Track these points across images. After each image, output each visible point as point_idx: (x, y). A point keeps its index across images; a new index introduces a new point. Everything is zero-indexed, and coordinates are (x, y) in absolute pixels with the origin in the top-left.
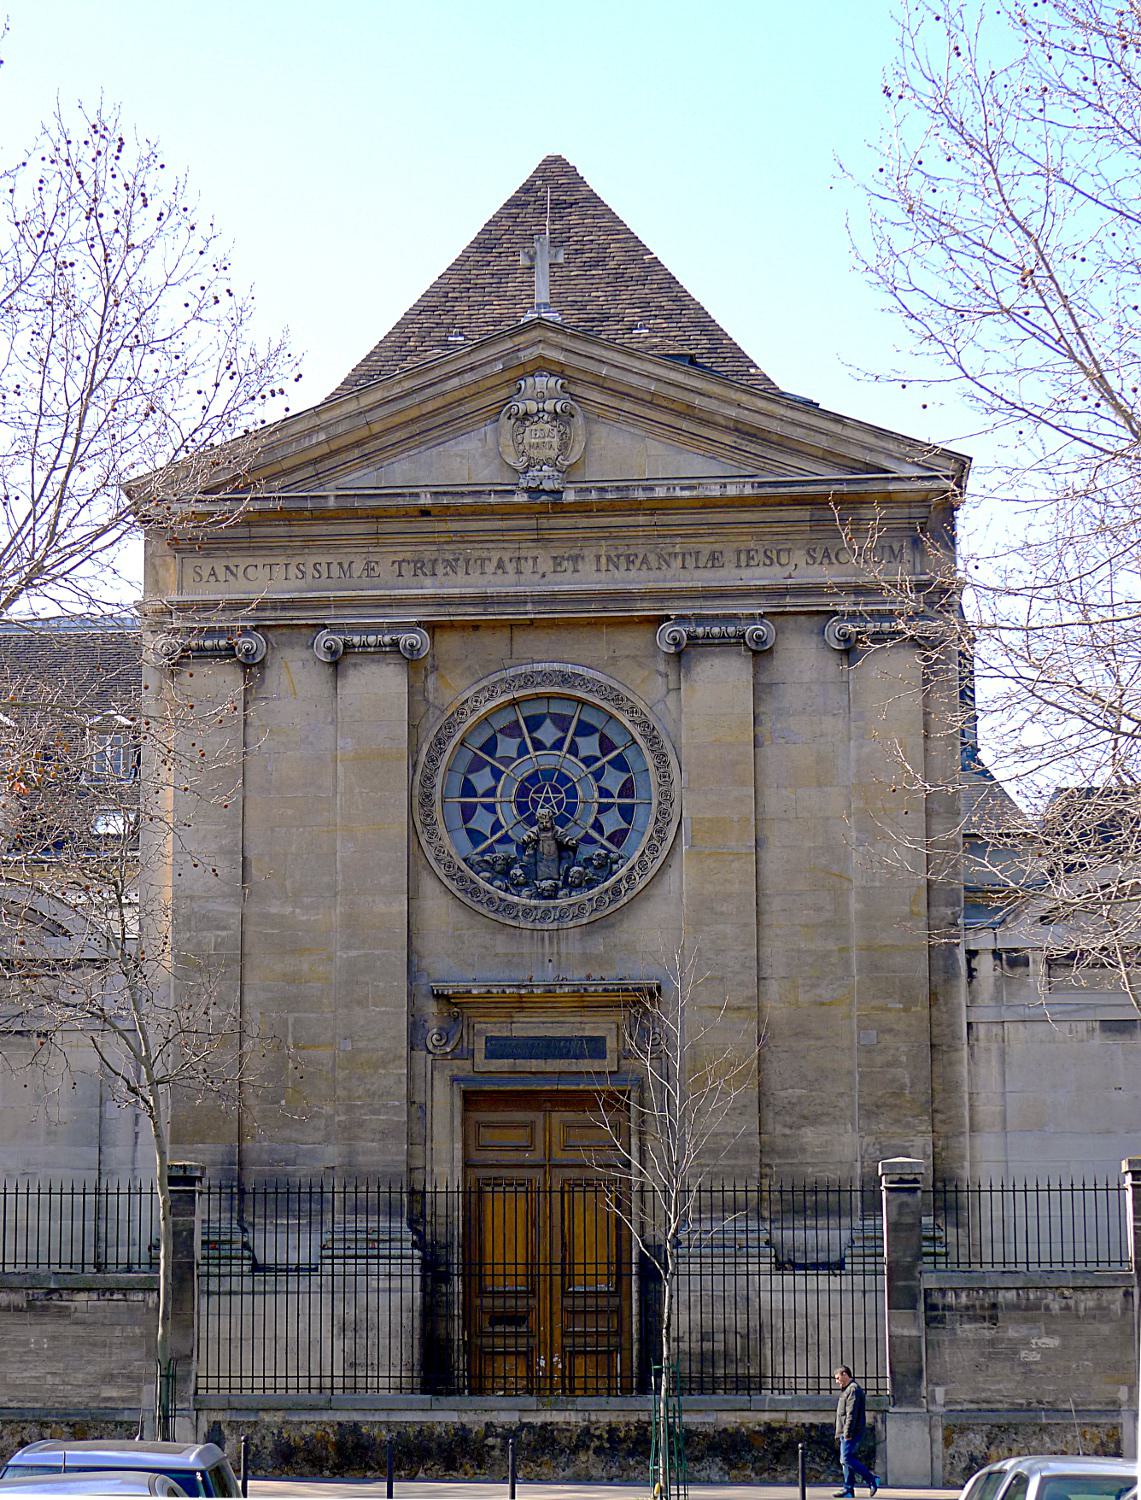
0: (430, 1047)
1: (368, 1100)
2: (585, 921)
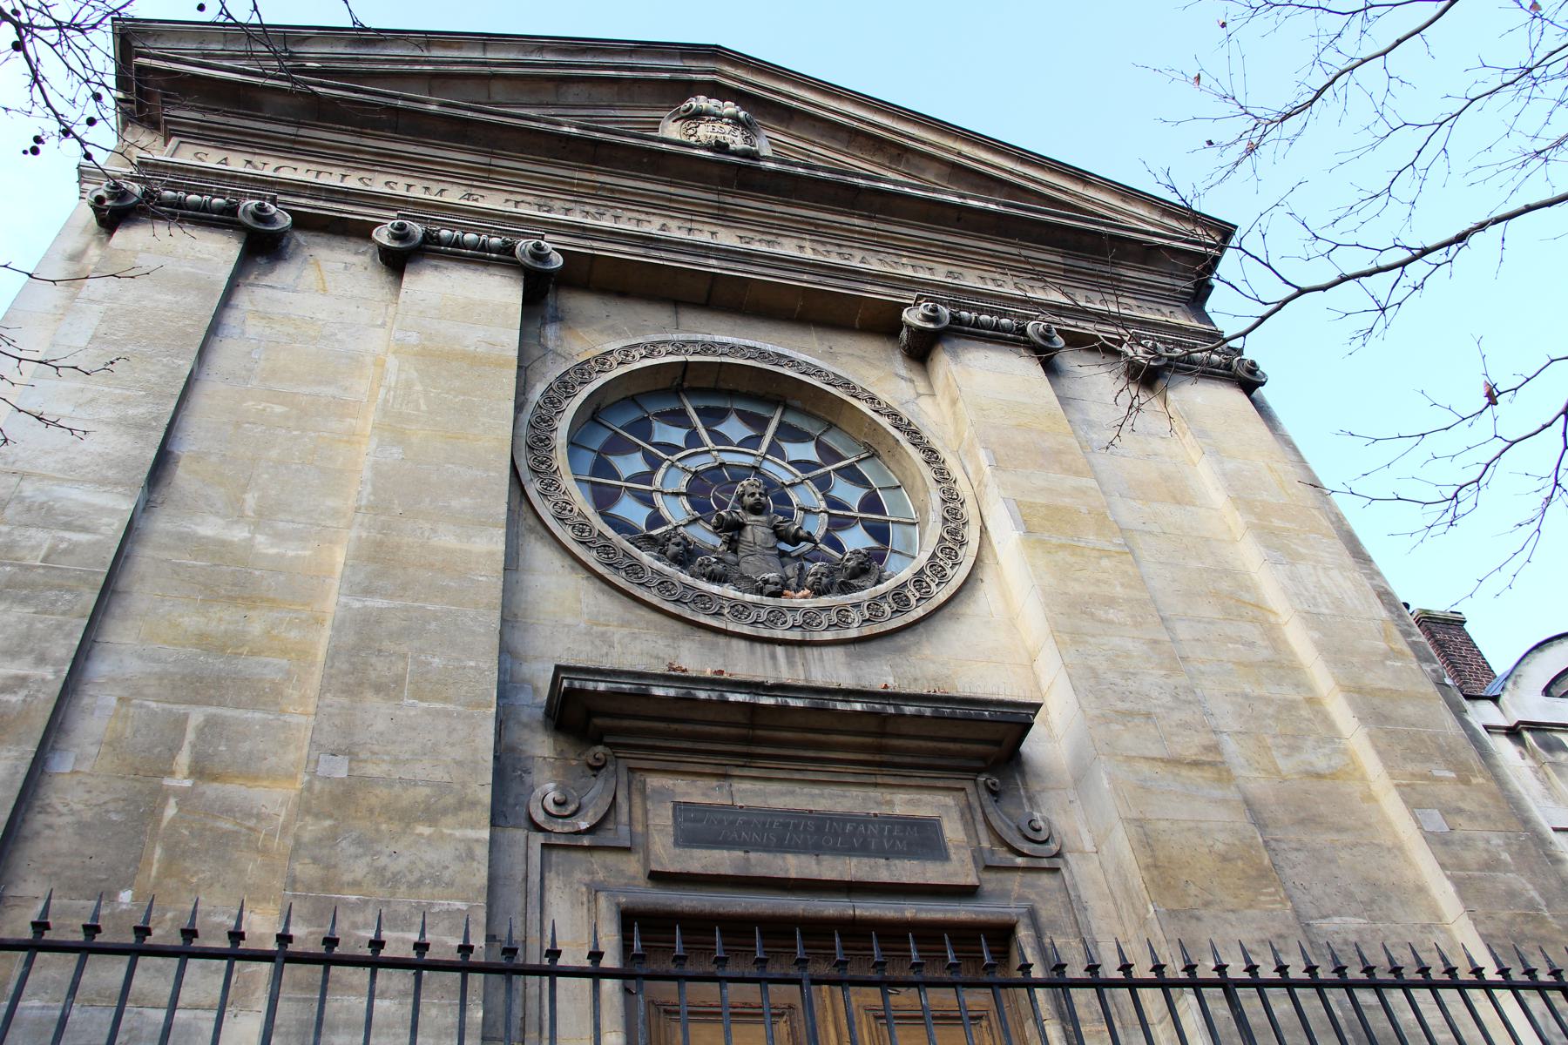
0: (540, 817)
1: (381, 893)
2: (853, 633)
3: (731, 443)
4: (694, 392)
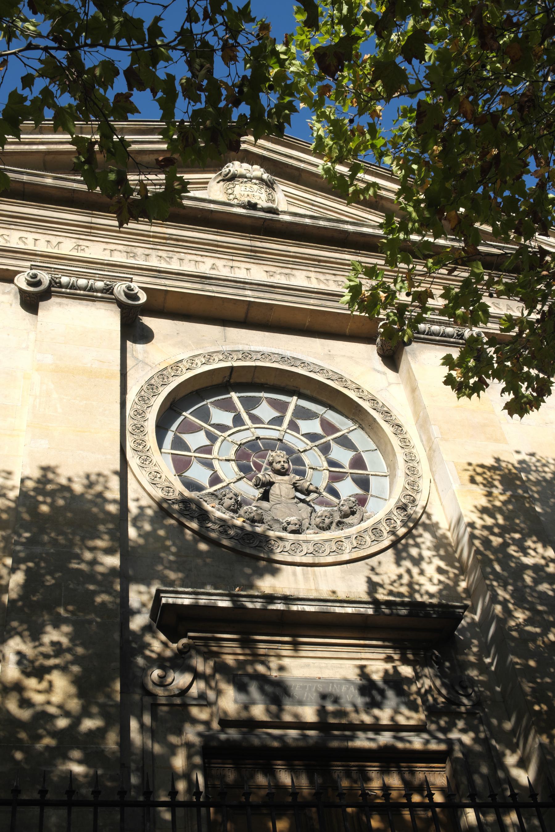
2: (346, 557)
3: (263, 423)
4: (239, 387)
